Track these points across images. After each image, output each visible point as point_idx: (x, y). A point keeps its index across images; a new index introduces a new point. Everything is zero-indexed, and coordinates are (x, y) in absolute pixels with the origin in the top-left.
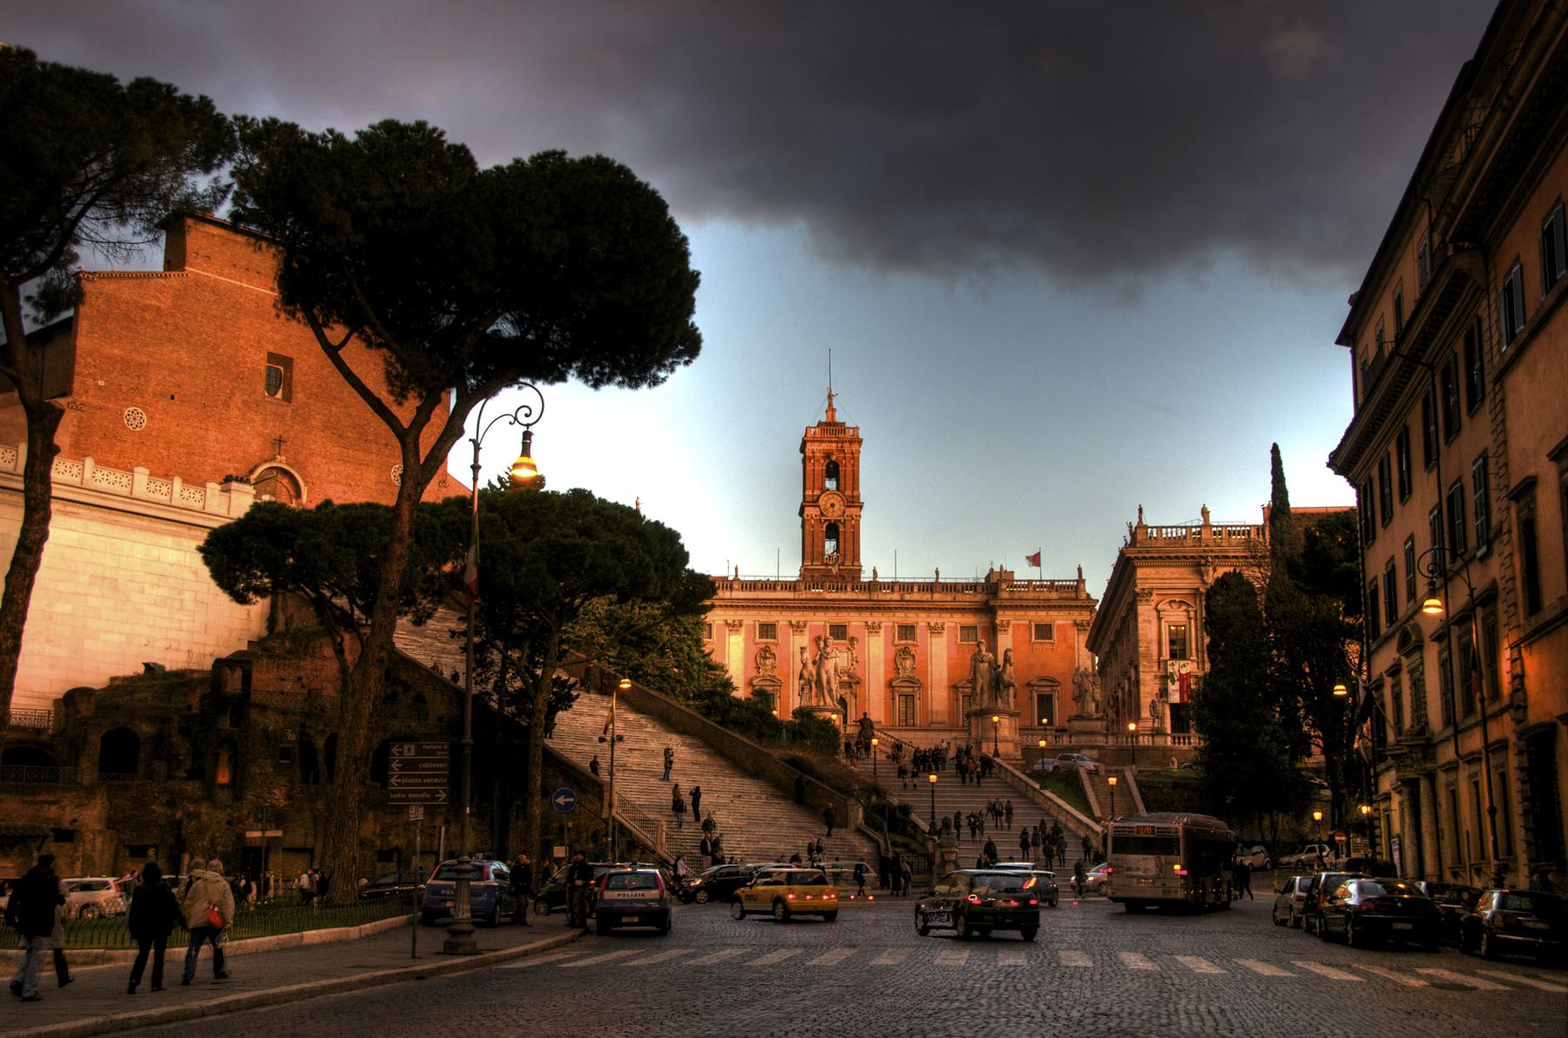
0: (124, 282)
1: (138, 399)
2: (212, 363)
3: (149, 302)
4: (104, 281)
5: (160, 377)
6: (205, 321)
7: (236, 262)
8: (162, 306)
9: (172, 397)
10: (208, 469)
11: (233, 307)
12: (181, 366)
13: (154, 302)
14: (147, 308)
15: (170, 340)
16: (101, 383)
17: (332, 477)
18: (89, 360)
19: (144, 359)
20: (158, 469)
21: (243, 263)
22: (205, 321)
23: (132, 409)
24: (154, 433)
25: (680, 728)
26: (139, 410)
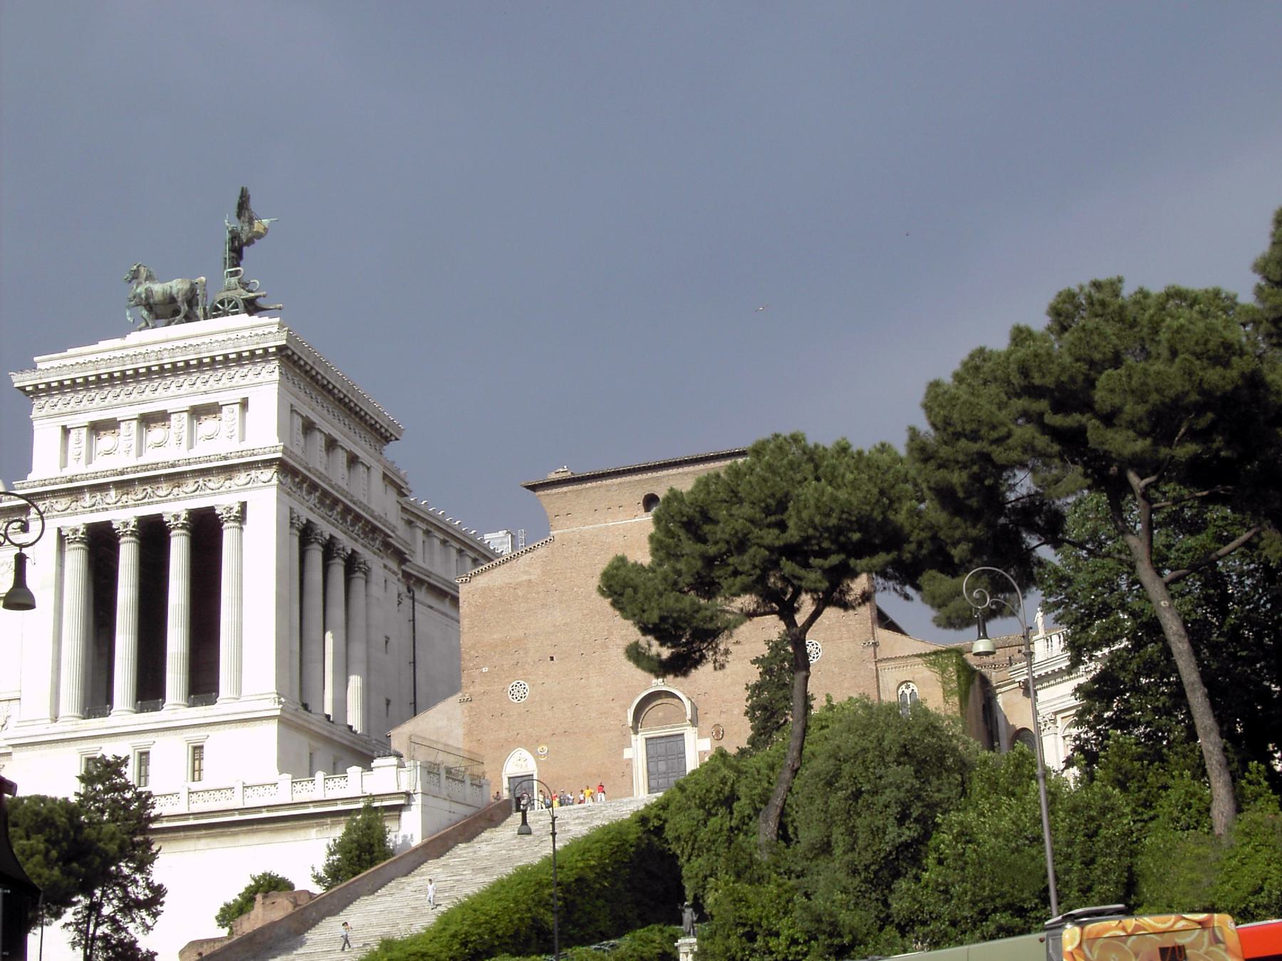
0: (496, 570)
1: (520, 672)
2: (585, 612)
3: (520, 580)
4: (478, 578)
5: (537, 645)
6: (574, 575)
7: (597, 507)
8: (532, 577)
9: (552, 659)
10: (594, 715)
11: (602, 550)
12: (554, 626)
13: (525, 578)
14: (520, 584)
15: (543, 606)
16: (485, 670)
17: (729, 680)
18: (473, 652)
19: (521, 633)
20: (545, 730)
21: (603, 505)
22: (574, 575)
23: (515, 683)
24: (537, 699)
25: (513, 950)
26: (522, 682)
